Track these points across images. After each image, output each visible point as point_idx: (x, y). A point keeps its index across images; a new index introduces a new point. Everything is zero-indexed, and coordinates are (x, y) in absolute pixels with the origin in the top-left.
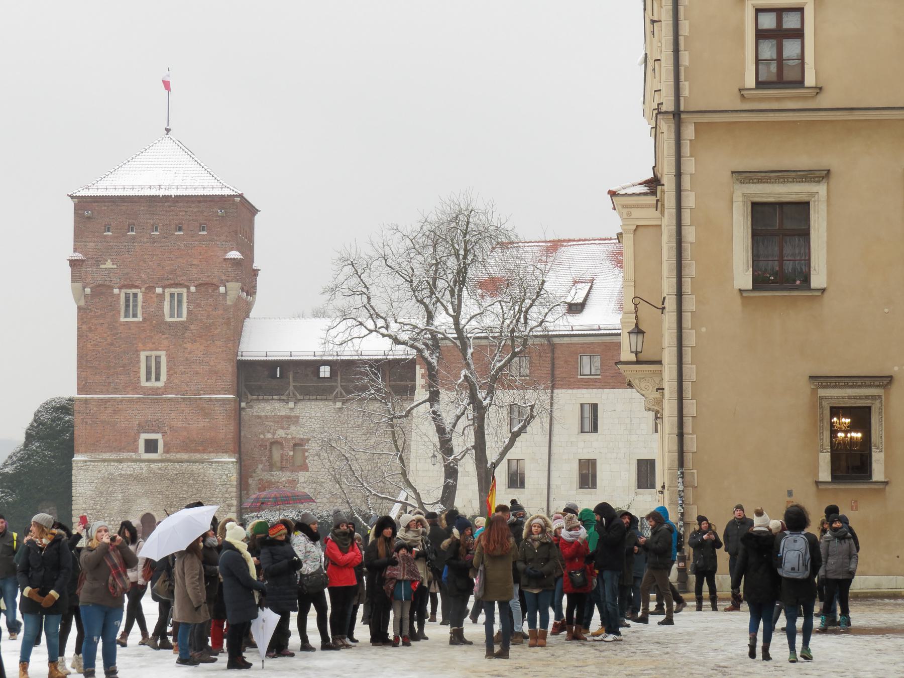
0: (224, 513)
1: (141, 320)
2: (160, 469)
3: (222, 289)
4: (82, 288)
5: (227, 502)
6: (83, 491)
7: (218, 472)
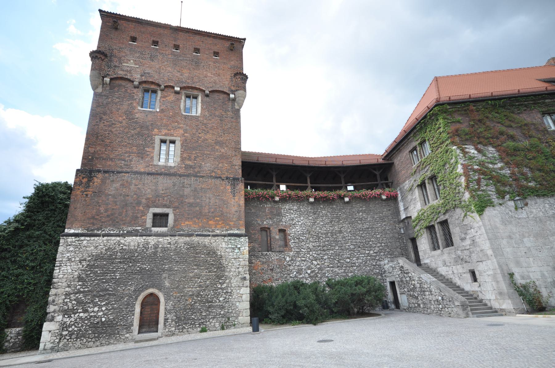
0: (238, 288)
1: (158, 110)
2: (170, 243)
3: (232, 96)
7: (230, 246)
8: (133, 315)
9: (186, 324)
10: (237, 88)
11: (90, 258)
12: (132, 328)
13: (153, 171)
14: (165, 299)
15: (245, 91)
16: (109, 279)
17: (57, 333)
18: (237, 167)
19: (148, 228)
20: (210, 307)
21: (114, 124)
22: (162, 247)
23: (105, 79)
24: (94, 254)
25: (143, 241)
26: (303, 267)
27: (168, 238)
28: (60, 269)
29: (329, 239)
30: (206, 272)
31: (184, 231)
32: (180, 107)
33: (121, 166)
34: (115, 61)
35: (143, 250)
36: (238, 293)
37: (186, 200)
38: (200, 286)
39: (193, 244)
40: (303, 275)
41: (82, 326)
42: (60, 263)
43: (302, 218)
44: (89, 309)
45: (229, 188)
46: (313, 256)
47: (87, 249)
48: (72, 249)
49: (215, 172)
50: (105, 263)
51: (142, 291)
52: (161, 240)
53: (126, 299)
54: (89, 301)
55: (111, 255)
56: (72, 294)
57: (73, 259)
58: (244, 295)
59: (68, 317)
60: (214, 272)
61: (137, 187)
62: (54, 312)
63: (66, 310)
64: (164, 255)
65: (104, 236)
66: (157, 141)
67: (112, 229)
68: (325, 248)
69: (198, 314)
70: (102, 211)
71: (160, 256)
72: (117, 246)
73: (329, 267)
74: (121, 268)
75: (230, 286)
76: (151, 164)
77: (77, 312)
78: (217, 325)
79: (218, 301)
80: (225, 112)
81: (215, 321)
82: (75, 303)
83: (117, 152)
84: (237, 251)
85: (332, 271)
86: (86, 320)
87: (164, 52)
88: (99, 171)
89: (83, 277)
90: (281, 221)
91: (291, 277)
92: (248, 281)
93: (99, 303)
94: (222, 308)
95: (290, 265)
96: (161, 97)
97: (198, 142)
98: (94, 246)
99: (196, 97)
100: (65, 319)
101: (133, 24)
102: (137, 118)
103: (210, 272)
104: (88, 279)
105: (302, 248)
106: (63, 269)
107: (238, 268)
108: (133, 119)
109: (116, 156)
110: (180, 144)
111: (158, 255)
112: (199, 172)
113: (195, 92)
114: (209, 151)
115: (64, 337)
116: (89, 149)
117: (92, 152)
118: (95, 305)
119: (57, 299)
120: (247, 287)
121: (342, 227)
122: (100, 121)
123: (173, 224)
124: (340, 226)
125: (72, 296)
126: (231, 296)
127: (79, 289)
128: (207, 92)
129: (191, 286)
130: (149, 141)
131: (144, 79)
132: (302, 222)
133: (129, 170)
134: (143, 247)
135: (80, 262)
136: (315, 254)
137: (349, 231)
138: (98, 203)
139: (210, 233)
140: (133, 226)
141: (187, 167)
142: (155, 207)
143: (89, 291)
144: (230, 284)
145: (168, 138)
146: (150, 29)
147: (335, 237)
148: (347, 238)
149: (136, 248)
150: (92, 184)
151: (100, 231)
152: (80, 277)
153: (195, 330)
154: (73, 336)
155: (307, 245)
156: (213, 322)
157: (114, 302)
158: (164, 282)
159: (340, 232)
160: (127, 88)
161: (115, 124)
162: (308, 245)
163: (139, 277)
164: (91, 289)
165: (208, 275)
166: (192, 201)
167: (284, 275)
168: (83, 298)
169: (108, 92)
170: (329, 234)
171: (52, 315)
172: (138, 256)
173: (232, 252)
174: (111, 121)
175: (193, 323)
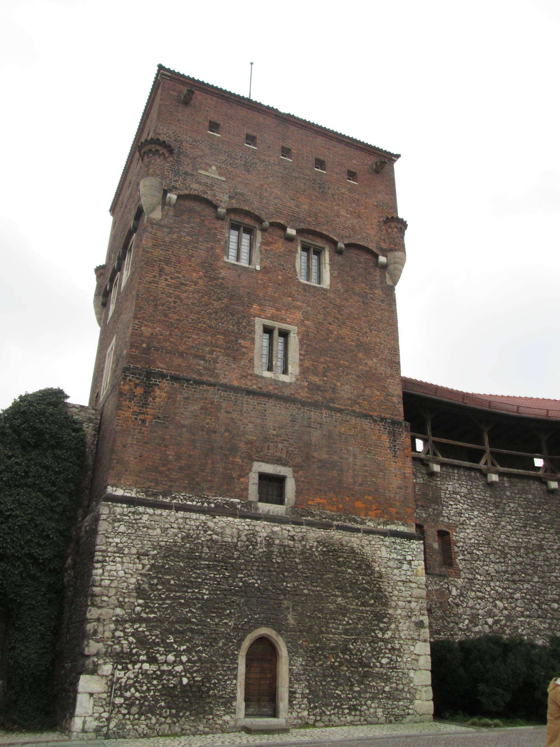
0: (410, 642)
1: (258, 268)
2: (292, 538)
3: (382, 259)
4: (162, 192)
5: (413, 619)
6: (121, 573)
7: (394, 556)
8: (236, 677)
9: (326, 705)
10: (393, 246)
11: (155, 552)
12: (234, 703)
13: (255, 387)
14: (289, 652)
15: (405, 253)
16: (190, 598)
17: (105, 699)
18: (395, 400)
19: (251, 502)
20: (366, 676)
21: (182, 284)
22: (279, 545)
23: (169, 195)
24: (163, 544)
25: (246, 527)
26: (480, 612)
27: (289, 527)
28: (103, 567)
29: (521, 559)
30: (357, 605)
31: (313, 515)
32: (294, 267)
33: (199, 370)
34: (186, 163)
35: (247, 546)
36: (411, 653)
37: (315, 454)
38: (346, 632)
39: (333, 545)
40: (480, 627)
41: (148, 690)
42: (104, 556)
43: (476, 513)
44: (158, 655)
45: (385, 439)
46: (497, 591)
47: (150, 531)
48: (122, 529)
49: (359, 404)
50: (182, 564)
51: (249, 631)
52: (276, 529)
53: (220, 644)
54: (157, 640)
55: (192, 551)
56: (126, 621)
57: (126, 551)
58: (421, 657)
59: (123, 669)
60: (372, 605)
61: (230, 416)
62: (97, 655)
63: (118, 654)
64: (285, 561)
65: (179, 508)
66: (259, 329)
67: (190, 497)
68: (516, 577)
69: (347, 688)
70: (171, 457)
71: (277, 562)
72: (202, 532)
73: (523, 616)
74: (211, 579)
75: (397, 636)
76: (250, 372)
77: (138, 661)
78: (380, 712)
79: (378, 664)
80: (371, 289)
81: (377, 705)
82: (134, 641)
83: (191, 339)
84: (406, 567)
85: (529, 623)
86: (155, 679)
87: (267, 159)
88: (163, 376)
89: (144, 590)
90: (440, 514)
91: (460, 629)
92: (427, 630)
93: (176, 646)
94: (387, 679)
95: (457, 605)
96: (262, 243)
97: (327, 339)
98: (161, 528)
99: (318, 252)
100: (118, 672)
101: (214, 98)
102: (223, 279)
103: (363, 604)
104: (155, 595)
105: (478, 573)
106: (108, 568)
107: (410, 602)
108: (217, 279)
109: (189, 349)
110: (297, 340)
111: (274, 560)
112: (332, 400)
113: (319, 243)
114: (346, 361)
115: (117, 709)
116: (142, 328)
117: (148, 334)
118: (169, 649)
119: (101, 629)
120: (425, 641)
121: (543, 539)
122: (160, 275)
123: (294, 498)
124: (541, 536)
125: (127, 625)
126: (400, 657)
127: (139, 614)
128: (341, 245)
129: (333, 630)
130: (245, 327)
131: (235, 204)
132: (476, 520)
133: (212, 380)
134: (247, 540)
135: (138, 558)
136: (499, 587)
137: (555, 547)
138: (164, 440)
139: (359, 526)
140: (226, 496)
141: (314, 388)
142: (263, 461)
143: (156, 619)
144: (397, 633)
145: (278, 325)
146: (242, 112)
147: (531, 556)
148: (553, 561)
149: (235, 540)
150: (151, 399)
151: (169, 499)
152: (139, 588)
153: (342, 719)
154: (134, 710)
155: (484, 567)
156: (373, 705)
157: (200, 648)
158: (286, 616)
159: (541, 548)
160: (204, 216)
161: (186, 285)
162: (487, 568)
163: (243, 600)
164: (160, 616)
165: (361, 612)
166: (324, 456)
167: (448, 623)
168: (147, 633)
169: (171, 221)
170: (522, 550)
171: (94, 662)
172: (238, 558)
173: (397, 568)
174: (179, 278)
175: (338, 704)
